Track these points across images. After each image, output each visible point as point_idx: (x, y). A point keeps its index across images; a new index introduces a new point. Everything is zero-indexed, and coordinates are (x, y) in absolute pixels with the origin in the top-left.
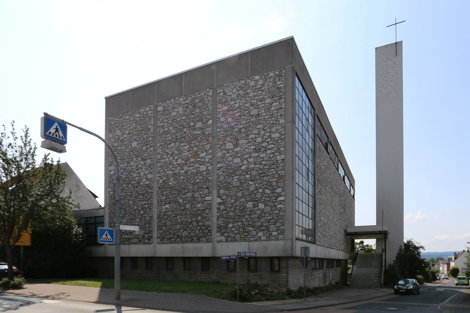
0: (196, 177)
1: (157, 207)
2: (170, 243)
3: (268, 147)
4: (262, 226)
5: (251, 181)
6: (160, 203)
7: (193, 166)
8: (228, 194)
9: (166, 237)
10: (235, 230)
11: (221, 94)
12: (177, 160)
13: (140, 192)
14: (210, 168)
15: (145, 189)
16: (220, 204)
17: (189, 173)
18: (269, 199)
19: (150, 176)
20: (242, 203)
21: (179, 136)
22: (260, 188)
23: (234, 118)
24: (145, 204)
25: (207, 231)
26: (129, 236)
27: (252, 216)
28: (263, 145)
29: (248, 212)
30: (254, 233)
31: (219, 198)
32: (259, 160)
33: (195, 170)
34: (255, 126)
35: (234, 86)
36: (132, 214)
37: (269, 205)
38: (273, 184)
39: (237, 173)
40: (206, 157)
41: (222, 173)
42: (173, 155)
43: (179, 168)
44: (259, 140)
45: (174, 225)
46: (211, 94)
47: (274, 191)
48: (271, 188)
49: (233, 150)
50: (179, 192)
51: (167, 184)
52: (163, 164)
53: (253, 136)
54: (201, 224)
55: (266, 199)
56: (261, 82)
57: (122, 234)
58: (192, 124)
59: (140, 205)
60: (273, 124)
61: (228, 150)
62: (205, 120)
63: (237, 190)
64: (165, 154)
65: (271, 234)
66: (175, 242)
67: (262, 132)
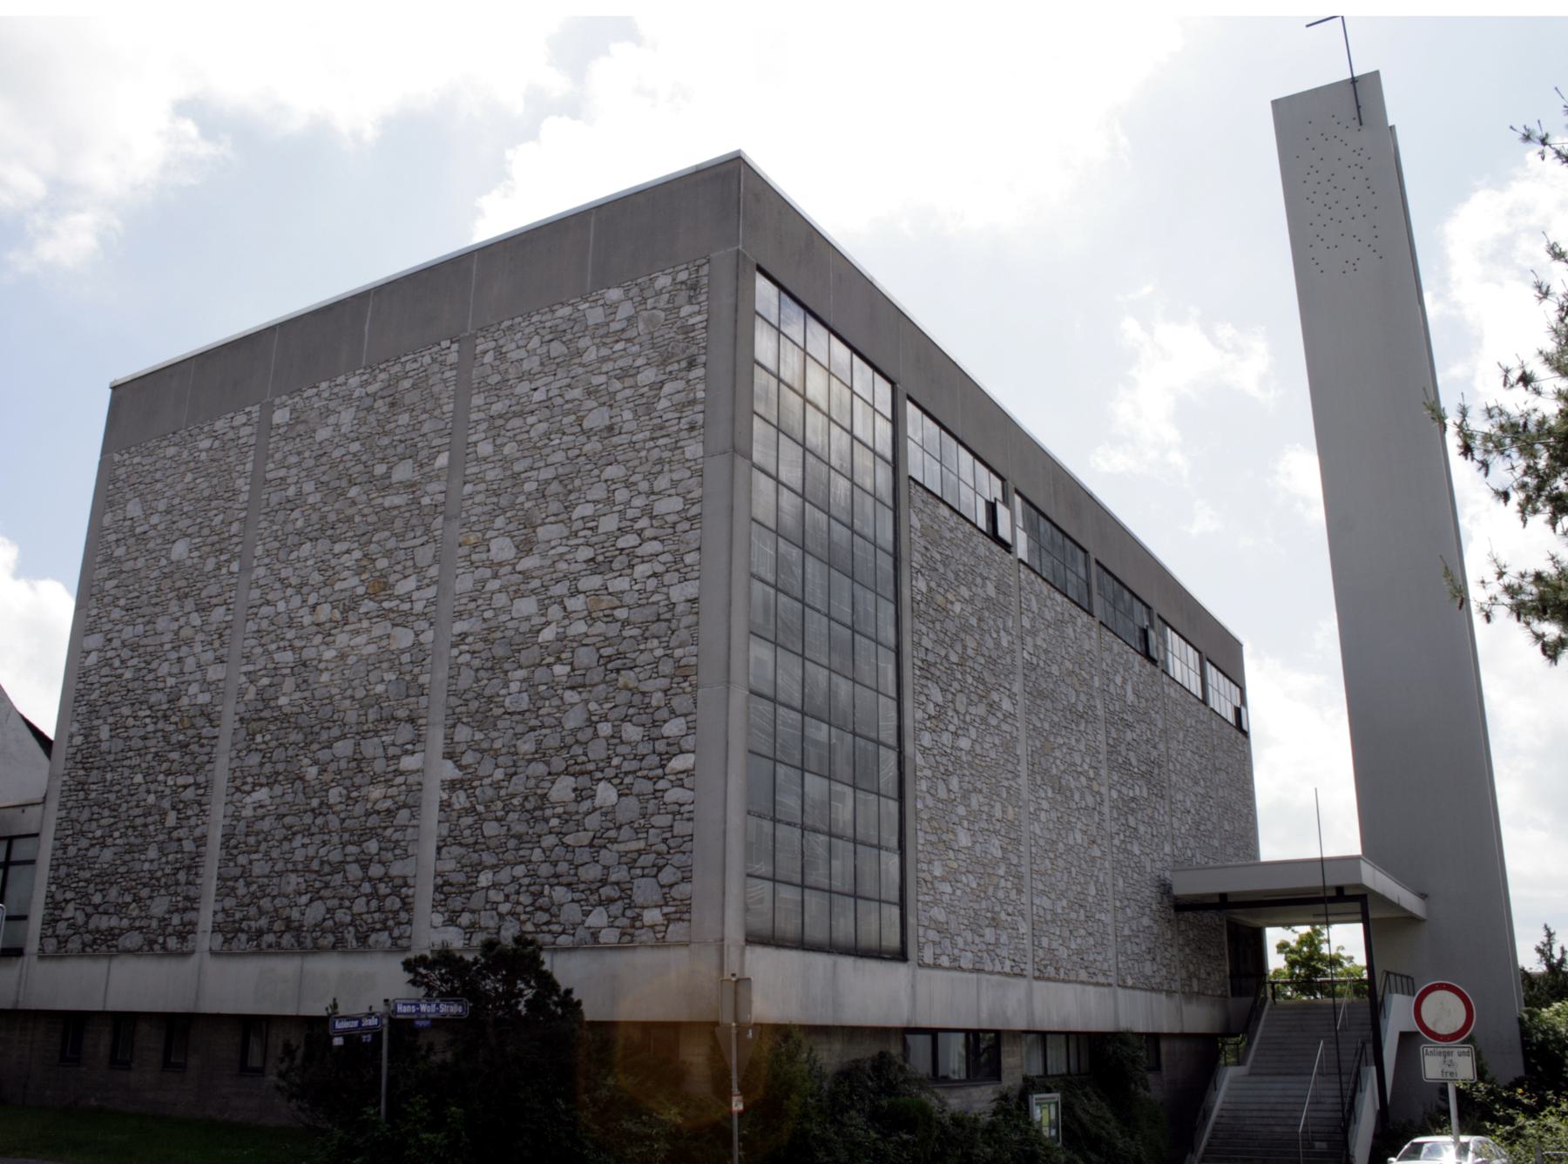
0: (373, 677)
1: (224, 799)
2: (259, 952)
3: (639, 552)
4: (604, 882)
5: (572, 688)
6: (238, 787)
7: (368, 631)
8: (485, 745)
9: (244, 925)
10: (501, 898)
11: (489, 358)
12: (314, 607)
13: (174, 739)
14: (428, 637)
15: (193, 726)
16: (452, 786)
17: (351, 660)
18: (634, 765)
19: (214, 673)
20: (532, 783)
21: (332, 517)
22: (604, 718)
23: (527, 445)
24: (185, 787)
25: (398, 904)
26: (114, 922)
27: (569, 840)
28: (621, 543)
29: (554, 822)
30: (571, 913)
31: (449, 764)
32: (607, 601)
33: (372, 649)
34: (596, 472)
35: (532, 328)
36: (135, 828)
37: (636, 789)
38: (654, 703)
39: (524, 657)
40: (415, 596)
41: (467, 657)
42: (305, 590)
43: (318, 639)
44: (609, 524)
45: (280, 874)
46: (453, 357)
47: (655, 733)
48: (644, 718)
49: (514, 565)
50: (310, 738)
51: (272, 704)
52: (265, 624)
53: (588, 510)
54: (376, 870)
55: (627, 766)
56: (626, 310)
57: (89, 910)
58: (380, 469)
59: (168, 791)
60: (660, 461)
61: (495, 566)
62: (424, 453)
63: (520, 729)
64: (277, 585)
65: (638, 917)
66: (277, 950)
67: (621, 495)
